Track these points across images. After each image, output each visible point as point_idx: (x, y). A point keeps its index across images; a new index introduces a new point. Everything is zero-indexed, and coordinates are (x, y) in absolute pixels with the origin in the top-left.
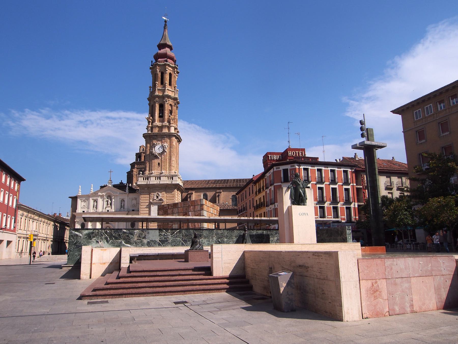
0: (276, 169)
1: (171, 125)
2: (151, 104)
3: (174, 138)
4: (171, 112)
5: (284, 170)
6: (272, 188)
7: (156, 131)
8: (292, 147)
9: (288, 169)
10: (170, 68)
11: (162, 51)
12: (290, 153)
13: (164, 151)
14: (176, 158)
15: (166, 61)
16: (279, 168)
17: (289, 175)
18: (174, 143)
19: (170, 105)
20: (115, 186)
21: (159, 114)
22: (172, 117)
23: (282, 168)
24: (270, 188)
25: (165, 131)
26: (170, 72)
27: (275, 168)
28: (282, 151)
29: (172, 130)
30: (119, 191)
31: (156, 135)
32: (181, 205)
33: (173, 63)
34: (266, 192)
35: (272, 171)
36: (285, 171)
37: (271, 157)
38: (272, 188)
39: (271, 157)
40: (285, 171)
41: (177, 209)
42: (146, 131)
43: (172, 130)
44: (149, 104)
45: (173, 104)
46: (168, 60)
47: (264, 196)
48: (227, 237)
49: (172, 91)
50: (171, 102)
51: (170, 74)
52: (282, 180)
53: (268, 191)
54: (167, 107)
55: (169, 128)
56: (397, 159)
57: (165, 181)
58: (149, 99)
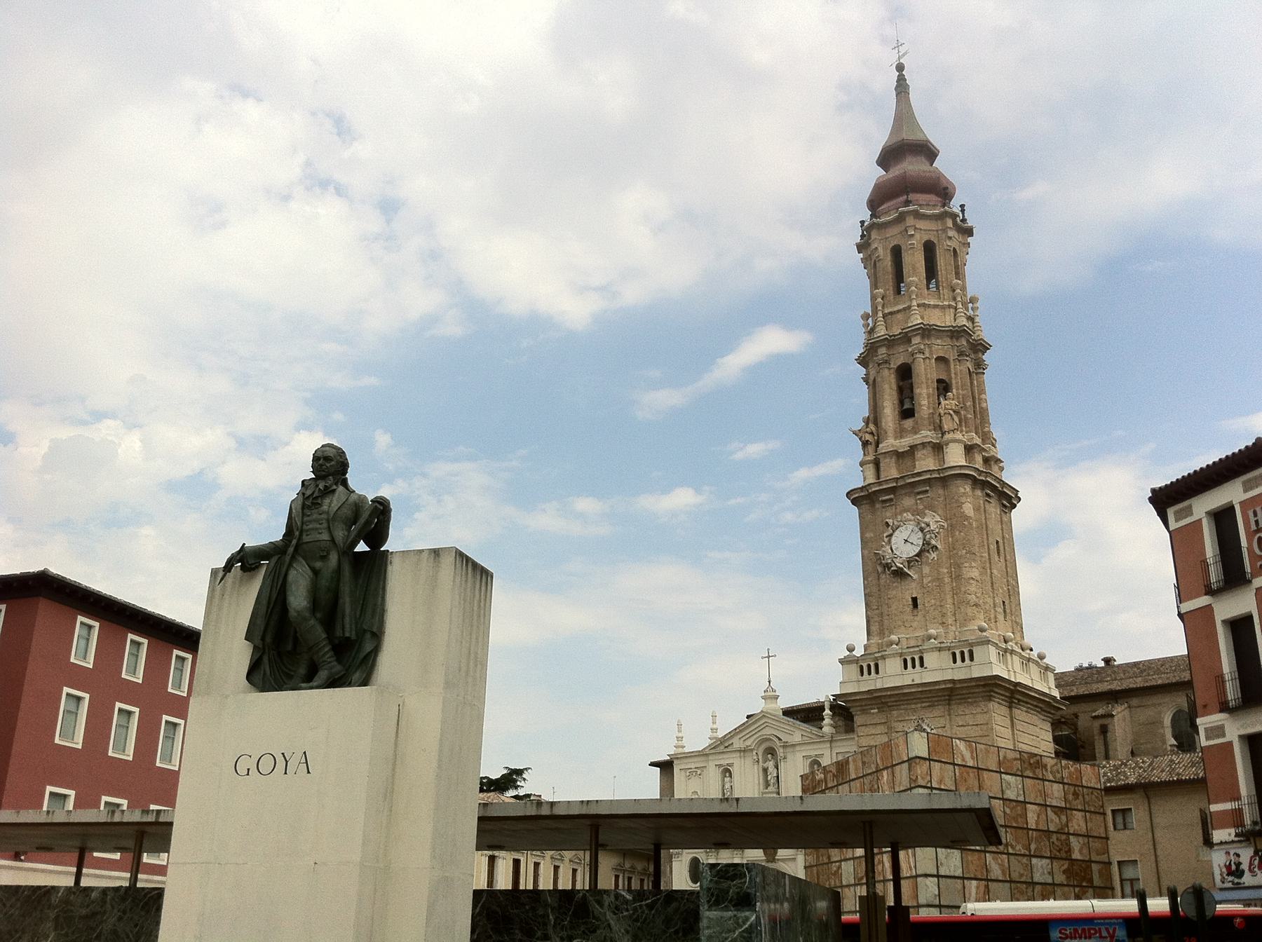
1: (947, 436)
2: (872, 378)
3: (966, 488)
4: (943, 387)
7: (891, 471)
10: (922, 224)
11: (896, 171)
13: (927, 547)
14: (987, 567)
15: (907, 203)
16: (1188, 511)
17: (1244, 543)
18: (968, 509)
19: (941, 359)
20: (789, 713)
21: (901, 403)
22: (949, 403)
25: (926, 463)
26: (926, 238)
29: (955, 456)
30: (797, 732)
31: (892, 490)
32: (856, 769)
33: (933, 198)
36: (1223, 518)
40: (1223, 518)
41: (846, 786)
42: (857, 480)
43: (955, 456)
44: (866, 380)
45: (952, 356)
46: (912, 196)
49: (943, 307)
50: (940, 346)
51: (929, 249)
52: (1215, 574)
54: (925, 374)
55: (938, 449)
57: (938, 669)
58: (863, 361)
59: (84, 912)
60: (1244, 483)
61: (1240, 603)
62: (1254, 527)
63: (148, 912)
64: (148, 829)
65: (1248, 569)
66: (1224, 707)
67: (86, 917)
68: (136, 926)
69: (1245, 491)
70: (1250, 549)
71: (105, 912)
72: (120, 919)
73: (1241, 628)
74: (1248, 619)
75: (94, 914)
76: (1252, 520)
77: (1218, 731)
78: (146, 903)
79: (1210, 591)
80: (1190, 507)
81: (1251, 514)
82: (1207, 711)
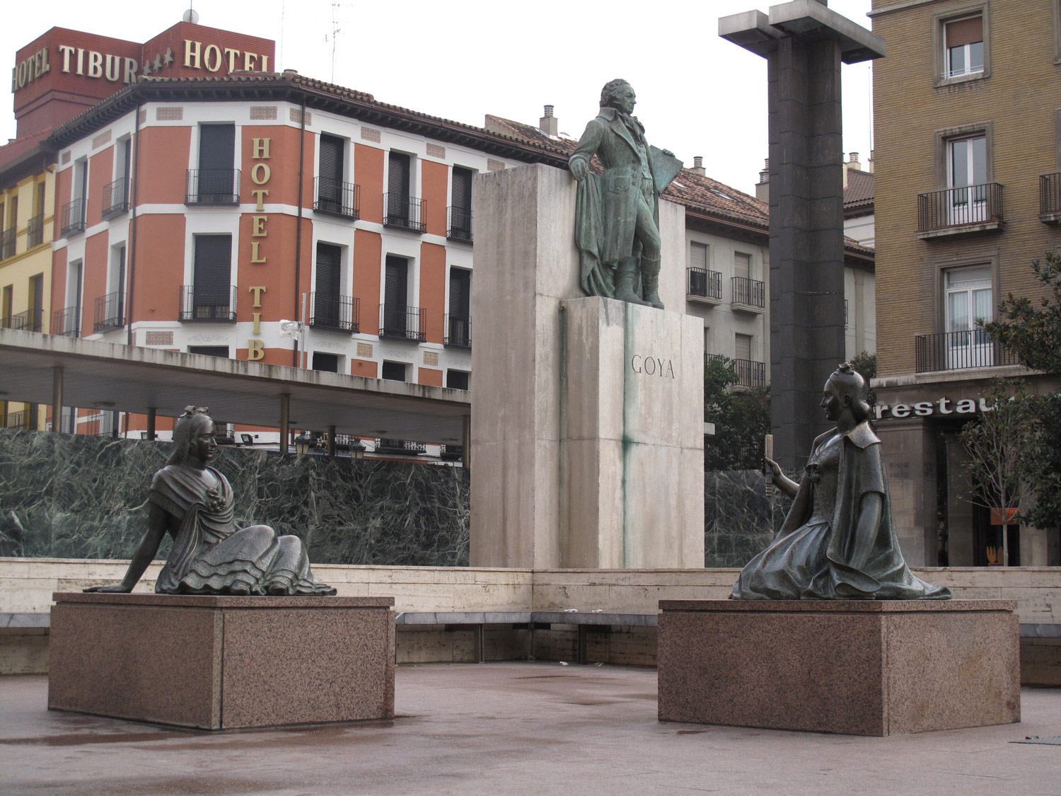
0: (161, 114)
5: (205, 128)
6: (119, 233)
8: (203, 20)
9: (229, 128)
12: (193, 54)
16: (178, 114)
23: (195, 115)
24: (91, 231)
27: (151, 113)
28: (141, 34)
34: (59, 257)
35: (125, 126)
36: (216, 136)
37: (74, 57)
38: (119, 233)
39: (74, 57)
40: (216, 136)
47: (36, 281)
48: (67, 497)
53: (76, 251)
56: (713, 172)
59: (26, 461)
60: (253, 109)
61: (223, 222)
62: (256, 155)
63: (107, 465)
64: (292, 389)
65: (236, 190)
66: (181, 320)
67: (29, 467)
68: (95, 481)
69: (252, 118)
70: (245, 174)
71: (54, 463)
72: (74, 472)
73: (212, 249)
74: (223, 240)
75: (40, 465)
76: (256, 148)
77: (167, 337)
78: (104, 456)
79: (188, 204)
80: (180, 110)
81: (256, 141)
82: (152, 314)
